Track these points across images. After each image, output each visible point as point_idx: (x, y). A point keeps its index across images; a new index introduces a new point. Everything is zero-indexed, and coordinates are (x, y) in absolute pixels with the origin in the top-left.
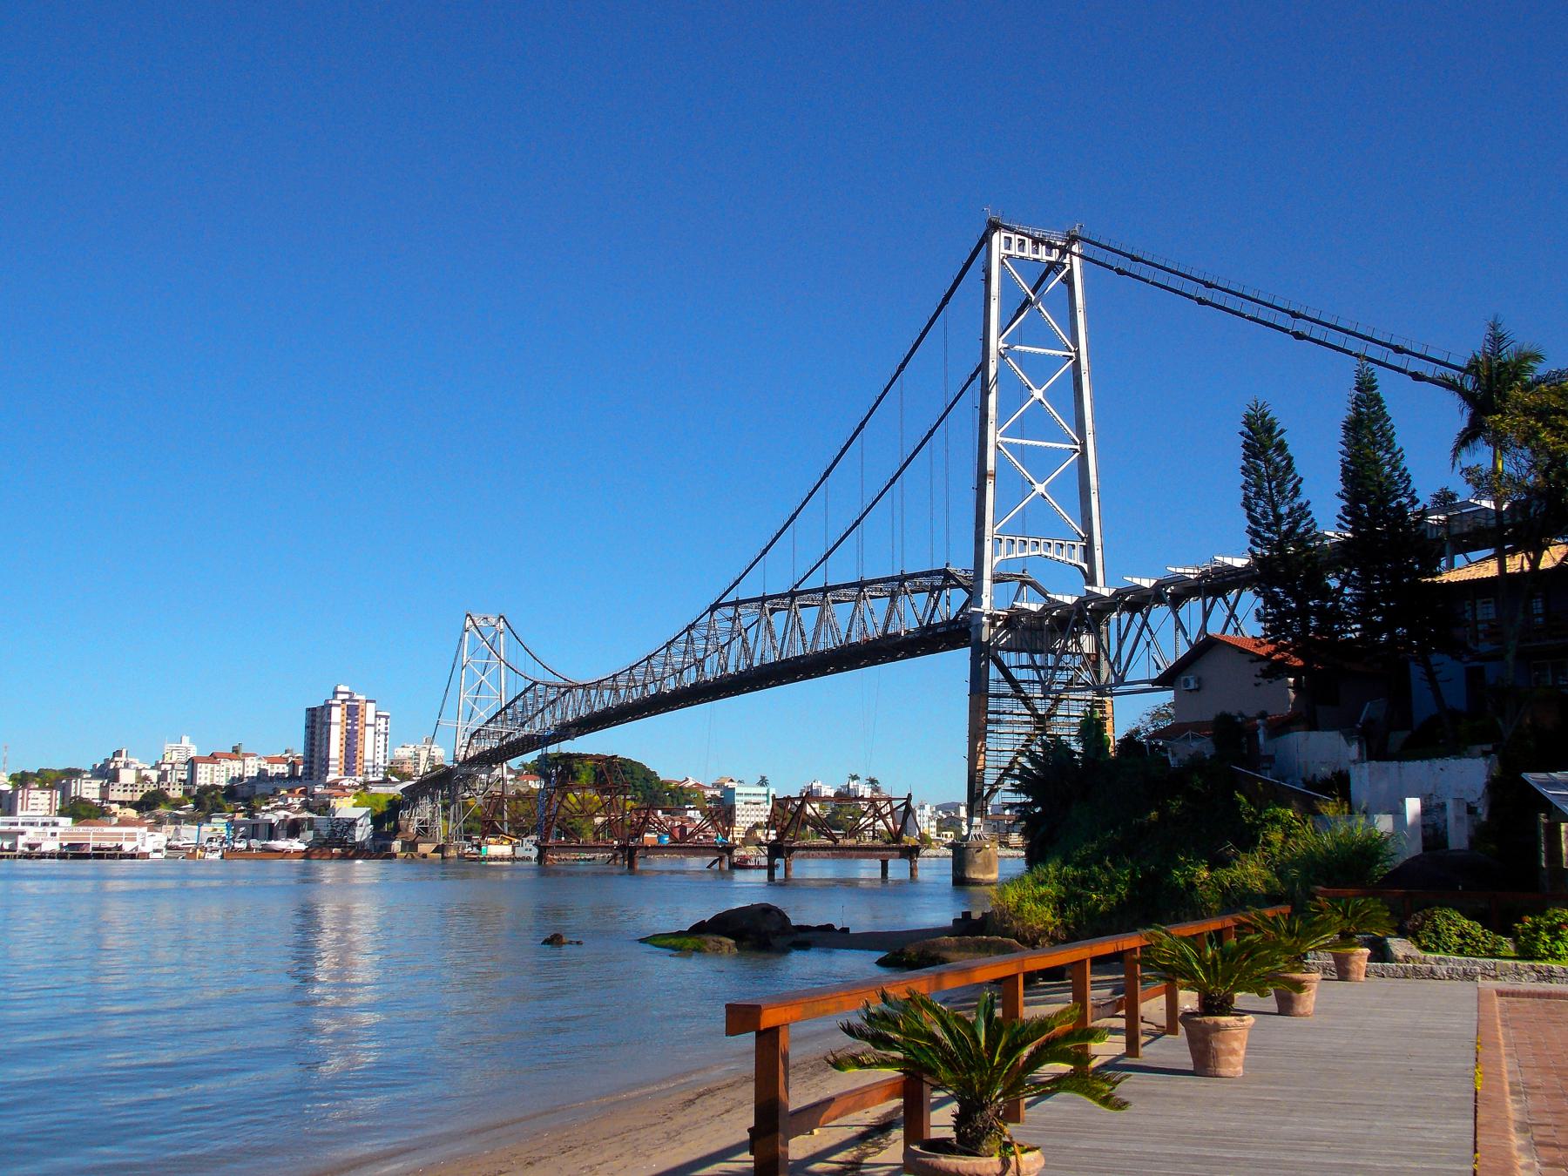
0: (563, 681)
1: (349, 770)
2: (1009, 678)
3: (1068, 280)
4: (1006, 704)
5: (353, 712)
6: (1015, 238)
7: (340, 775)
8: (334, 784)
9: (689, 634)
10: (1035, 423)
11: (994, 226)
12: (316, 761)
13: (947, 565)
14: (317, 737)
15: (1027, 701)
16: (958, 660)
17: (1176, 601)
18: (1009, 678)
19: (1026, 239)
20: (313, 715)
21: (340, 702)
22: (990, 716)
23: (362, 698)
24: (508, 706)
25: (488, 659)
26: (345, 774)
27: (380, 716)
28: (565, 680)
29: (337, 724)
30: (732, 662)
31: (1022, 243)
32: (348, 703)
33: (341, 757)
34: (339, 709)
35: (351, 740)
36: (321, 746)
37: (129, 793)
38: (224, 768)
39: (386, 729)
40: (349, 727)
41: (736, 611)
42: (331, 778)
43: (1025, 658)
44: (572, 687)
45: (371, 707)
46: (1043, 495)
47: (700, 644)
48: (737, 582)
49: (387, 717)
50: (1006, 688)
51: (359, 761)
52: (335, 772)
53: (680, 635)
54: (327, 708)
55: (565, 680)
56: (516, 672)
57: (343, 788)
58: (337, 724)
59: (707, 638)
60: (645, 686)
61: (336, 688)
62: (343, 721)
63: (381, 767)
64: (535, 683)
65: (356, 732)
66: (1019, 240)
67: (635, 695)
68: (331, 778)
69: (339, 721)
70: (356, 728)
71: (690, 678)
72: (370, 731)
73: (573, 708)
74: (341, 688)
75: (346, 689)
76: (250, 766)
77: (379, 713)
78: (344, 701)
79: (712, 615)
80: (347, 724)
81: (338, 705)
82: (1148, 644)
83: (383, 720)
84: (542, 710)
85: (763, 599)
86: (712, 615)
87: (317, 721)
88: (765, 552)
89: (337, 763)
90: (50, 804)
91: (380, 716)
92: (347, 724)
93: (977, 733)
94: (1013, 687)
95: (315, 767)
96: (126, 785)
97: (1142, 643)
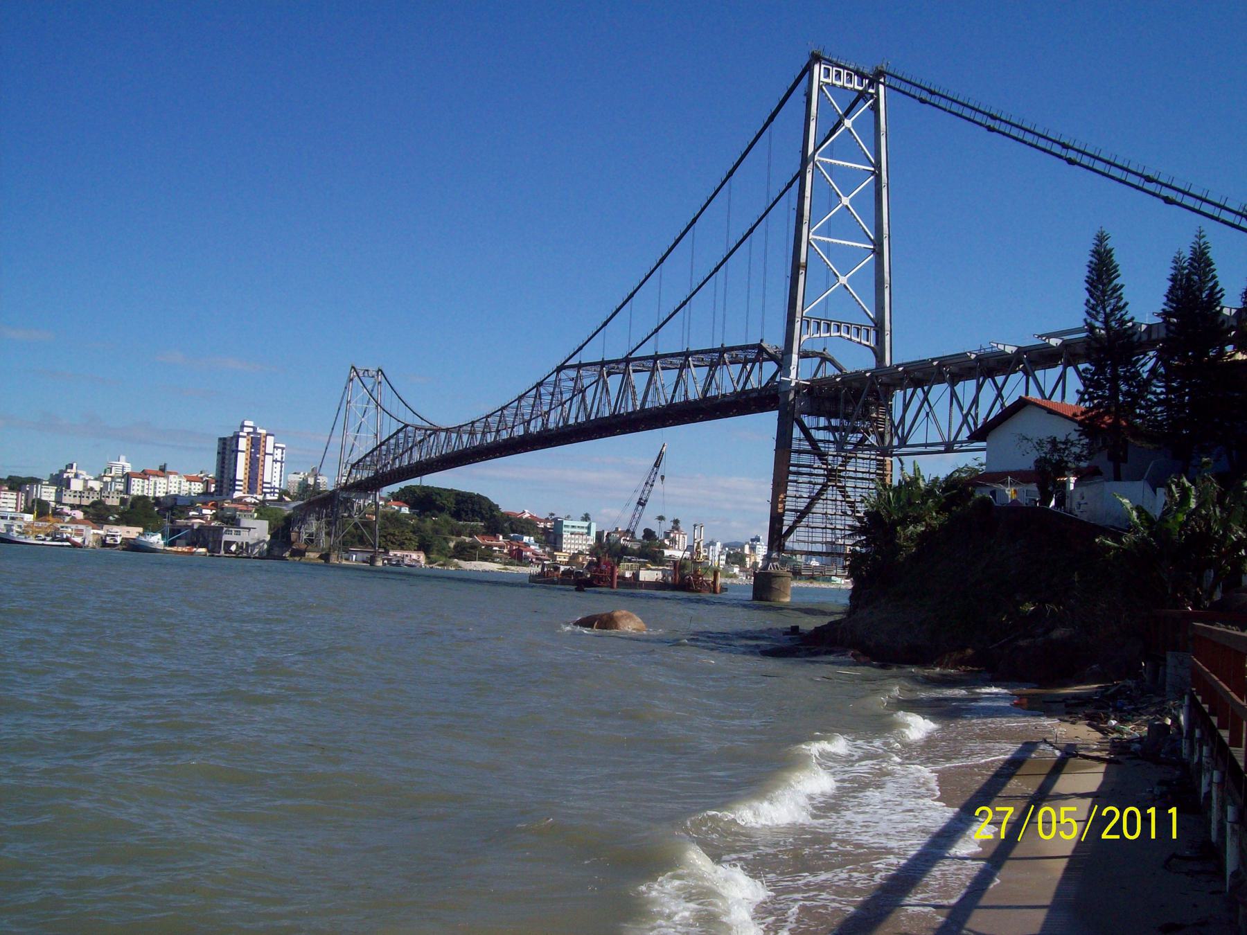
0: (429, 425)
1: (252, 486)
2: (808, 437)
3: (875, 108)
4: (806, 459)
5: (256, 443)
6: (833, 71)
7: (244, 493)
8: (240, 500)
9: (537, 390)
10: (841, 225)
11: (816, 58)
12: (225, 481)
13: (762, 341)
14: (226, 462)
15: (822, 456)
16: (770, 420)
18: (808, 437)
19: (842, 70)
20: (224, 444)
21: (245, 434)
22: (791, 468)
23: (264, 432)
24: (382, 444)
25: (368, 404)
26: (248, 492)
27: (277, 448)
28: (431, 424)
30: (573, 414)
31: (838, 75)
33: (245, 479)
34: (245, 439)
36: (229, 469)
37: (78, 498)
38: (153, 482)
39: (282, 458)
41: (579, 372)
42: (237, 495)
43: (822, 422)
44: (437, 430)
45: (270, 440)
46: (845, 286)
47: (547, 399)
48: (581, 348)
49: (283, 449)
50: (806, 445)
51: (260, 482)
52: (240, 490)
54: (237, 437)
55: (431, 424)
56: (391, 416)
57: (246, 504)
59: (553, 394)
60: (498, 431)
61: (243, 422)
63: (277, 488)
64: (406, 426)
66: (836, 71)
67: (490, 438)
68: (237, 495)
70: (258, 456)
71: (535, 427)
72: (269, 459)
73: (437, 447)
74: (246, 423)
75: (251, 423)
77: (277, 445)
78: (248, 433)
79: (557, 374)
80: (251, 452)
81: (244, 437)
82: (927, 414)
83: (280, 450)
84: (411, 448)
85: (603, 364)
86: (557, 374)
87: (227, 449)
88: (605, 324)
90: (17, 504)
91: (277, 448)
93: (779, 485)
94: (810, 445)
95: (225, 486)
96: (76, 492)
97: (923, 414)
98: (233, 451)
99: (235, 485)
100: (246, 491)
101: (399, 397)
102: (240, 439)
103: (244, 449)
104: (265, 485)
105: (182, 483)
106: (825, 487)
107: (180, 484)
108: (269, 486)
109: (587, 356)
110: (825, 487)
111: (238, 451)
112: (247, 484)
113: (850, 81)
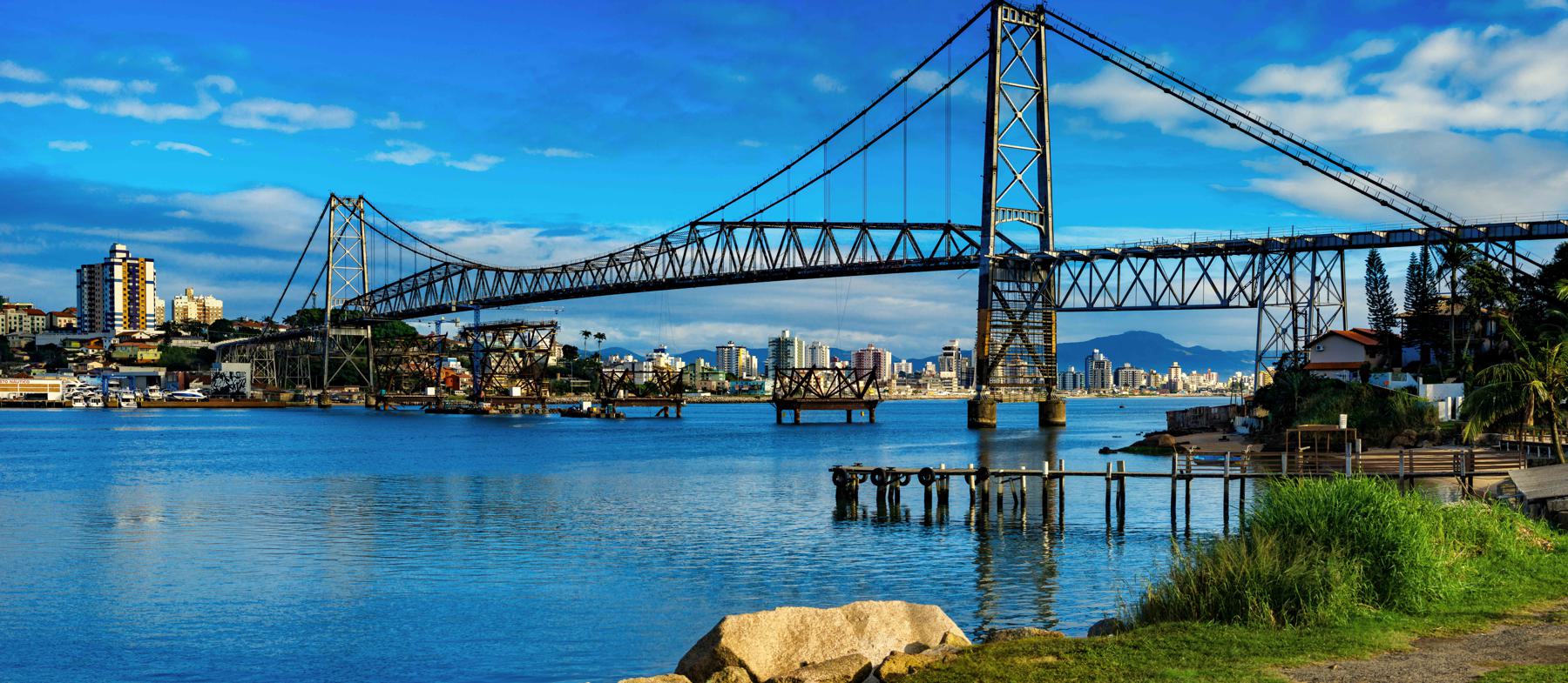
5: (133, 272)
7: (125, 328)
13: (949, 221)
17: (1118, 258)
21: (121, 261)
29: (120, 281)
32: (128, 261)
35: (134, 296)
40: (131, 284)
42: (119, 330)
43: (1013, 286)
45: (150, 265)
46: (1020, 181)
48: (723, 208)
52: (121, 325)
53: (656, 239)
54: (110, 266)
55: (463, 260)
58: (120, 281)
61: (114, 245)
62: (124, 278)
64: (447, 264)
65: (138, 288)
68: (119, 330)
69: (121, 278)
72: (150, 288)
74: (119, 247)
75: (123, 247)
76: (13, 318)
78: (124, 259)
80: (129, 281)
81: (120, 264)
89: (121, 317)
92: (129, 281)
98: (107, 281)
99: (114, 320)
100: (126, 325)
101: (401, 229)
102: (116, 267)
103: (121, 278)
104: (148, 318)
105: (24, 319)
106: (1012, 335)
107: (21, 318)
108: (153, 318)
109: (730, 215)
110: (1012, 335)
111: (113, 281)
112: (128, 318)
113: (1020, 19)
